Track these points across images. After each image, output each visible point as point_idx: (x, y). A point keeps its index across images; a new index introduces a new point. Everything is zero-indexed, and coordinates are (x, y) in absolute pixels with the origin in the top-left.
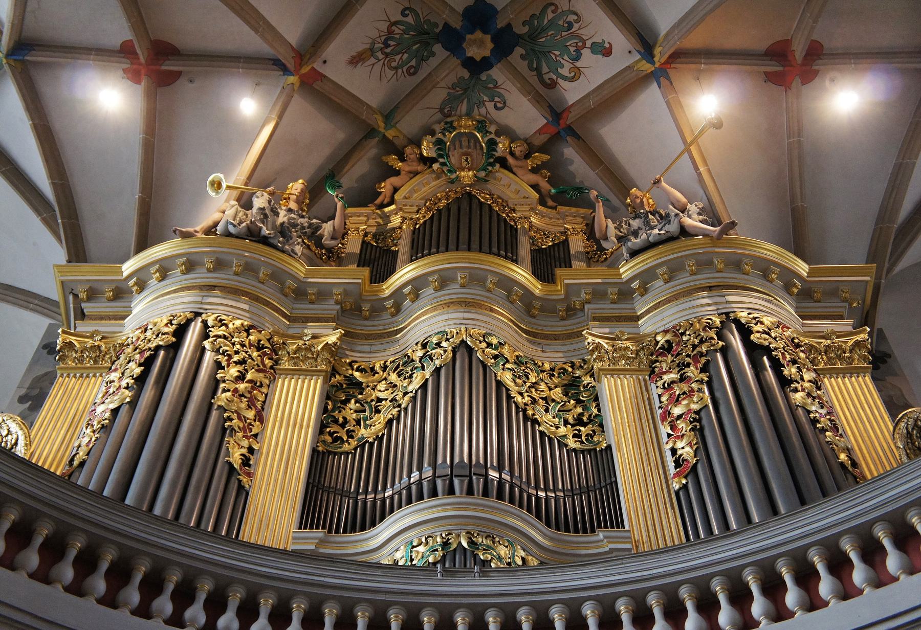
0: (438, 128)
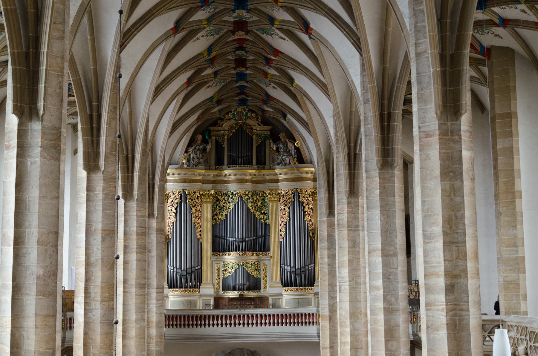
0: (233, 110)
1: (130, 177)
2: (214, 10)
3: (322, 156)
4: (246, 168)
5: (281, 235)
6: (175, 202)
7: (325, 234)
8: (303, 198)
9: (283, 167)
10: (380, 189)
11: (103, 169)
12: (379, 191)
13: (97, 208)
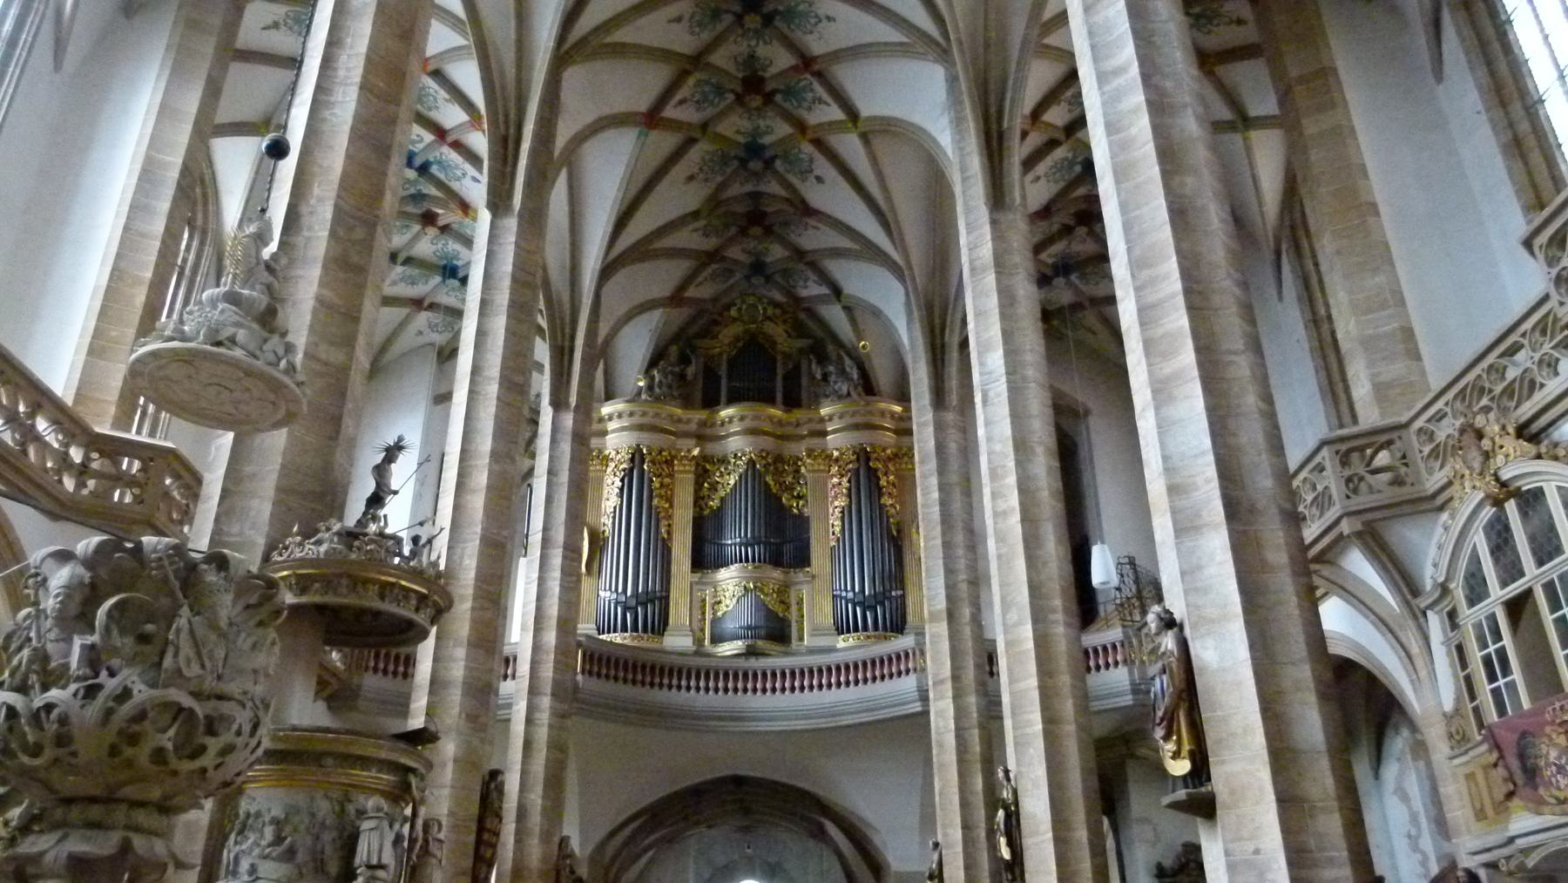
0: (738, 301)
7: (931, 444)
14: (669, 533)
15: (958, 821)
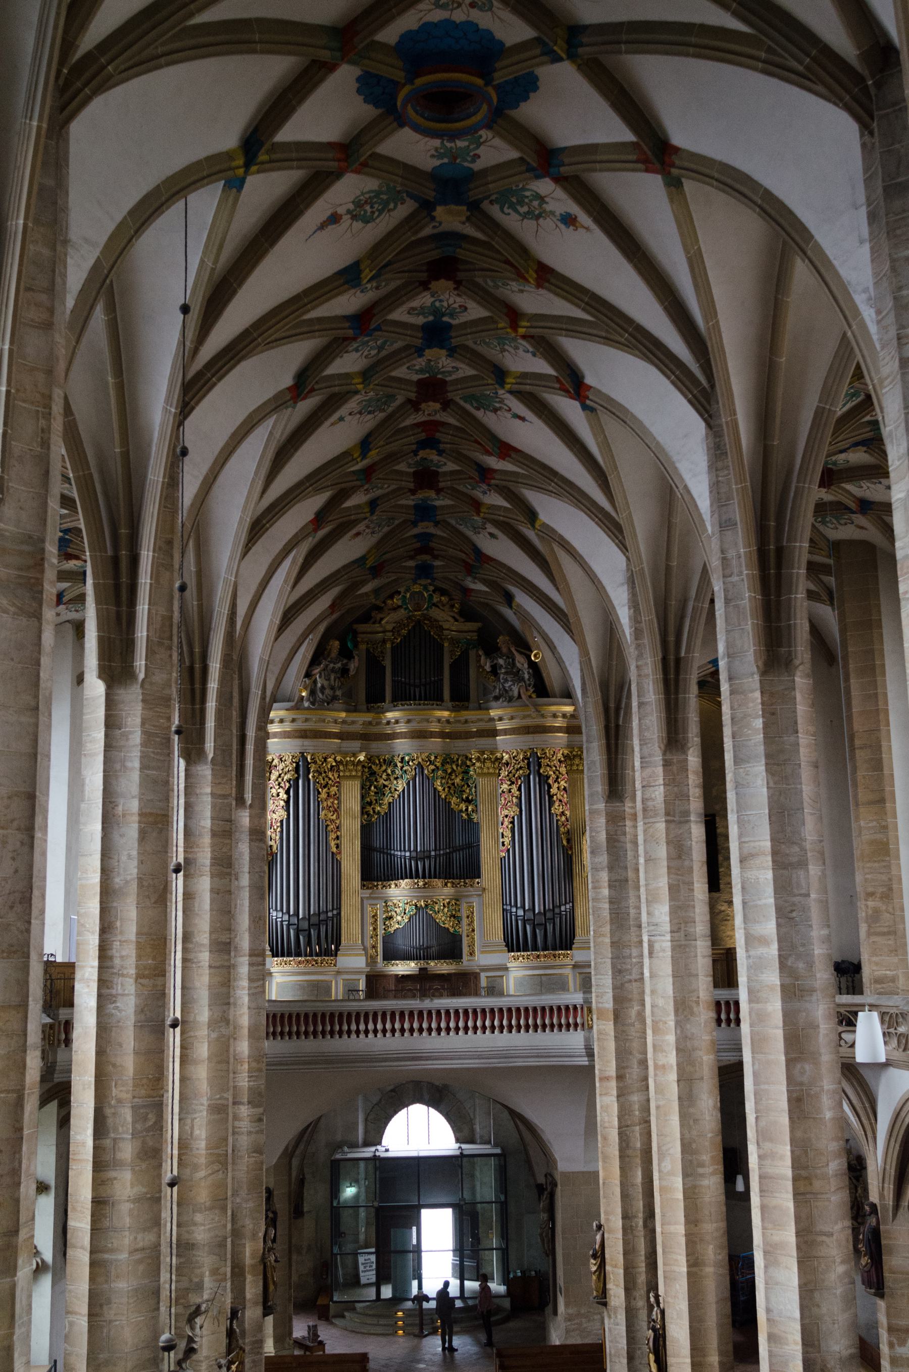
0: (402, 590)
1: (198, 712)
2: (379, 352)
3: (593, 674)
4: (429, 707)
5: (503, 845)
6: (286, 778)
7: (603, 836)
8: (548, 769)
9: (505, 703)
10: (763, 717)
11: (142, 676)
12: (761, 720)
13: (129, 764)
14: (338, 846)
15: (619, 1211)
